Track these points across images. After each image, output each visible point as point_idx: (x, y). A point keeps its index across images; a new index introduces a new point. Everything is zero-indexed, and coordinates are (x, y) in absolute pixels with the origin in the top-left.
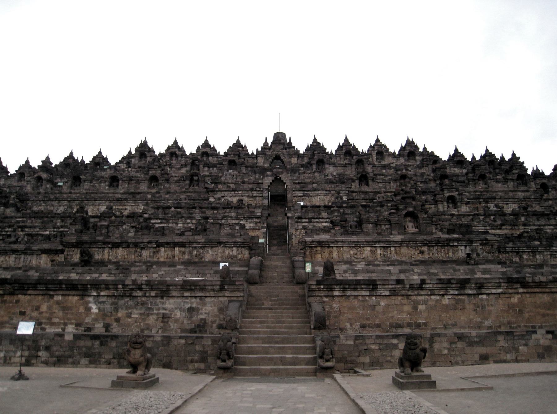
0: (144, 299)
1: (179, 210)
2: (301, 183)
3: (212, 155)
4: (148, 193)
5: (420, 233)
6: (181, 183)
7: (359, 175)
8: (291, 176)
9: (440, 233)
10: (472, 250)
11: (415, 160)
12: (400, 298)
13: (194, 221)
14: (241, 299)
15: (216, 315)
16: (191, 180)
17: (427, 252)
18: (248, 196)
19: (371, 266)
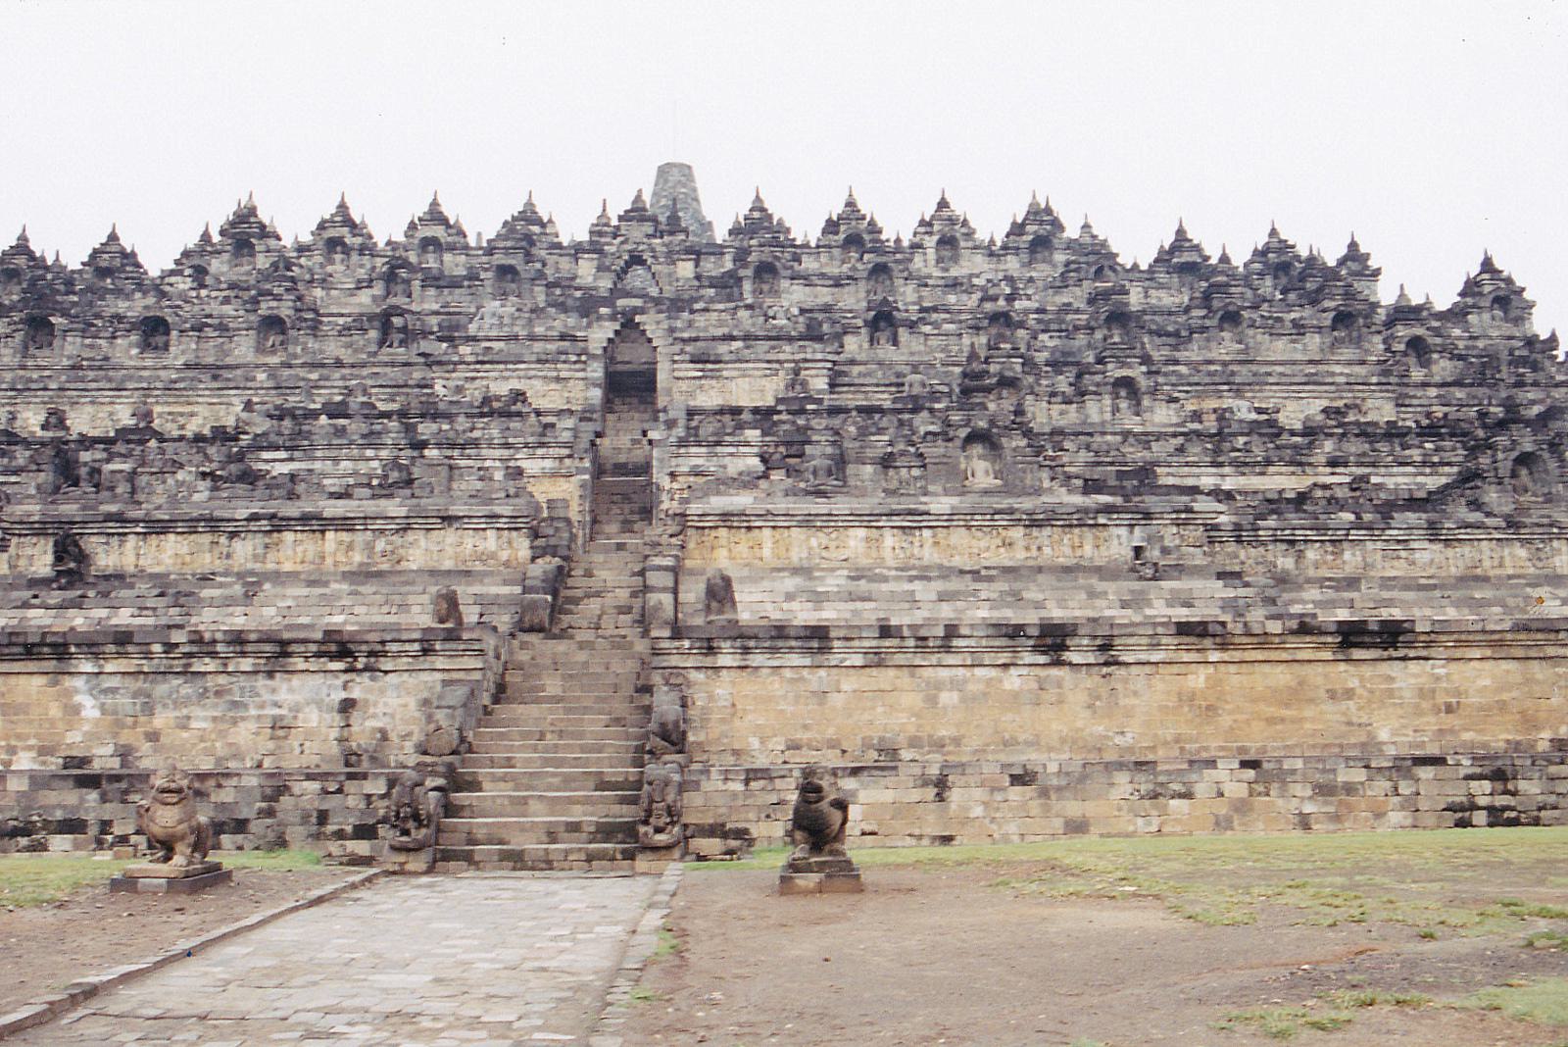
0: (222, 680)
1: (342, 422)
2: (696, 339)
3: (452, 248)
4: (257, 366)
5: (1007, 490)
6: (355, 338)
7: (873, 313)
8: (669, 318)
9: (1063, 490)
10: (1149, 539)
11: (1050, 262)
12: (892, 672)
13: (384, 453)
14: (477, 676)
15: (415, 718)
16: (386, 328)
17: (1021, 543)
19: (863, 582)
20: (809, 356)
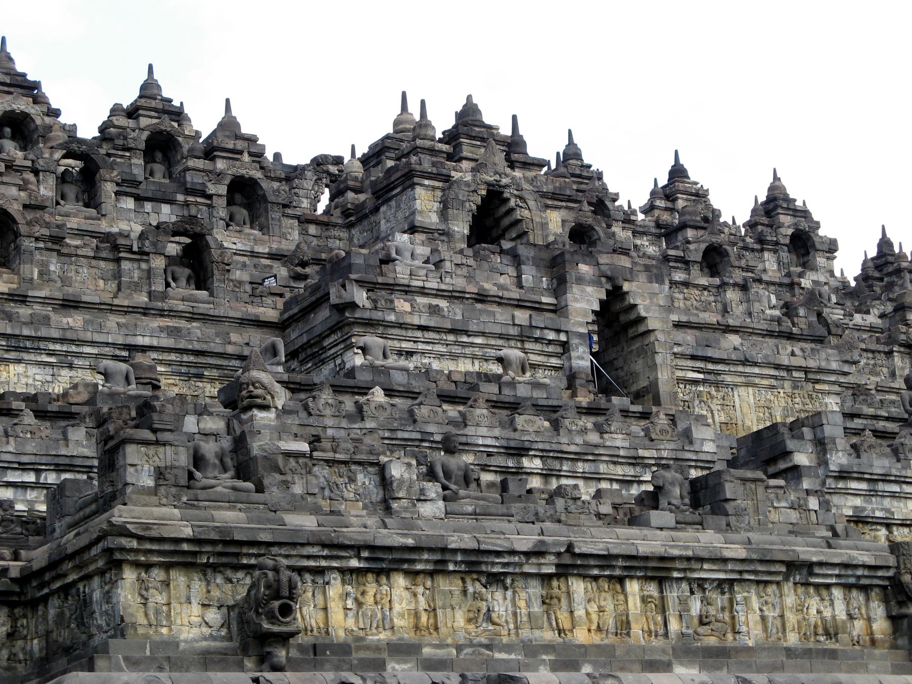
20: (824, 364)
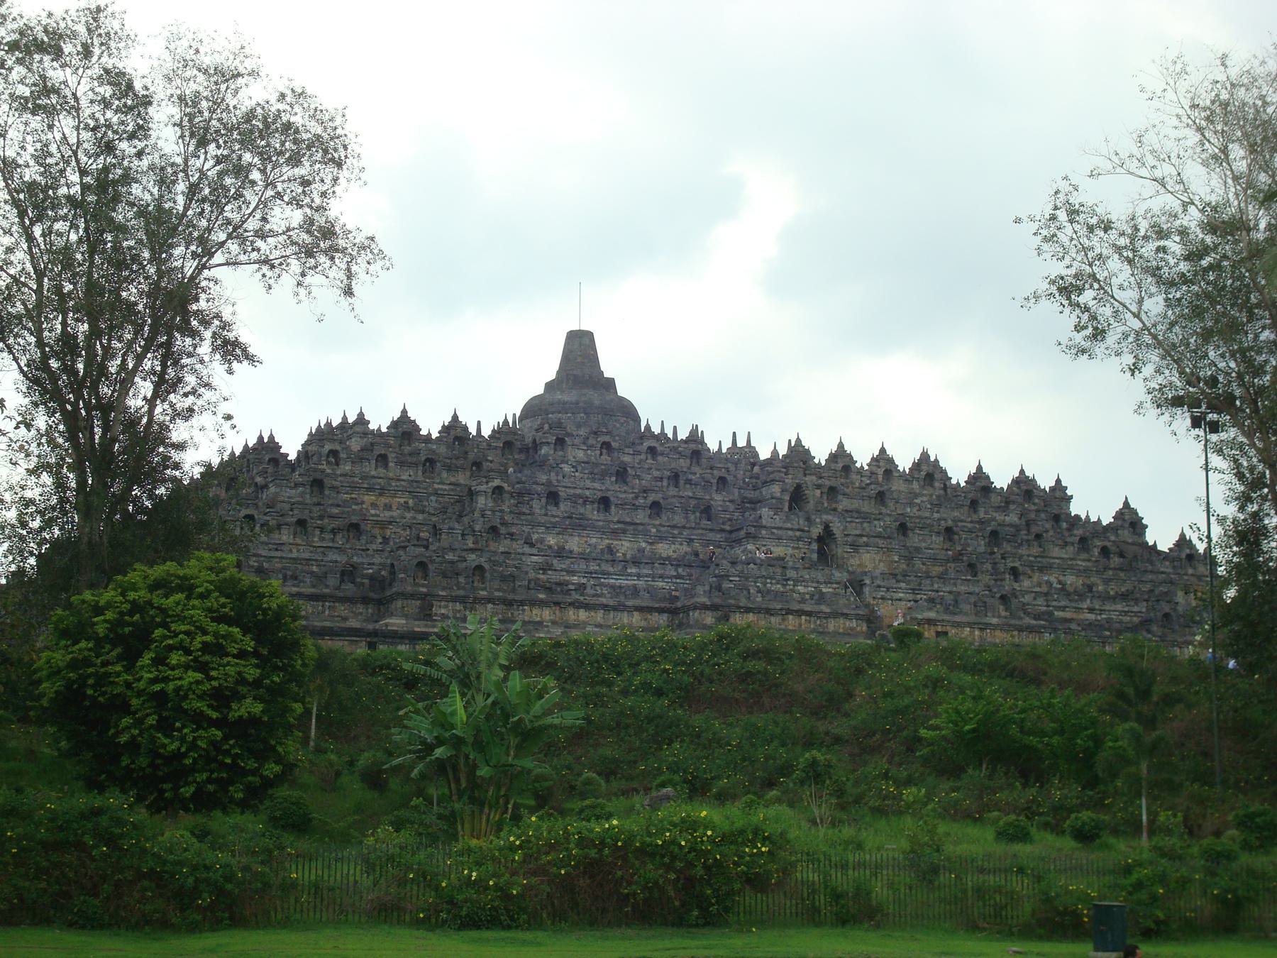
11: (932, 486)
18: (793, 548)
